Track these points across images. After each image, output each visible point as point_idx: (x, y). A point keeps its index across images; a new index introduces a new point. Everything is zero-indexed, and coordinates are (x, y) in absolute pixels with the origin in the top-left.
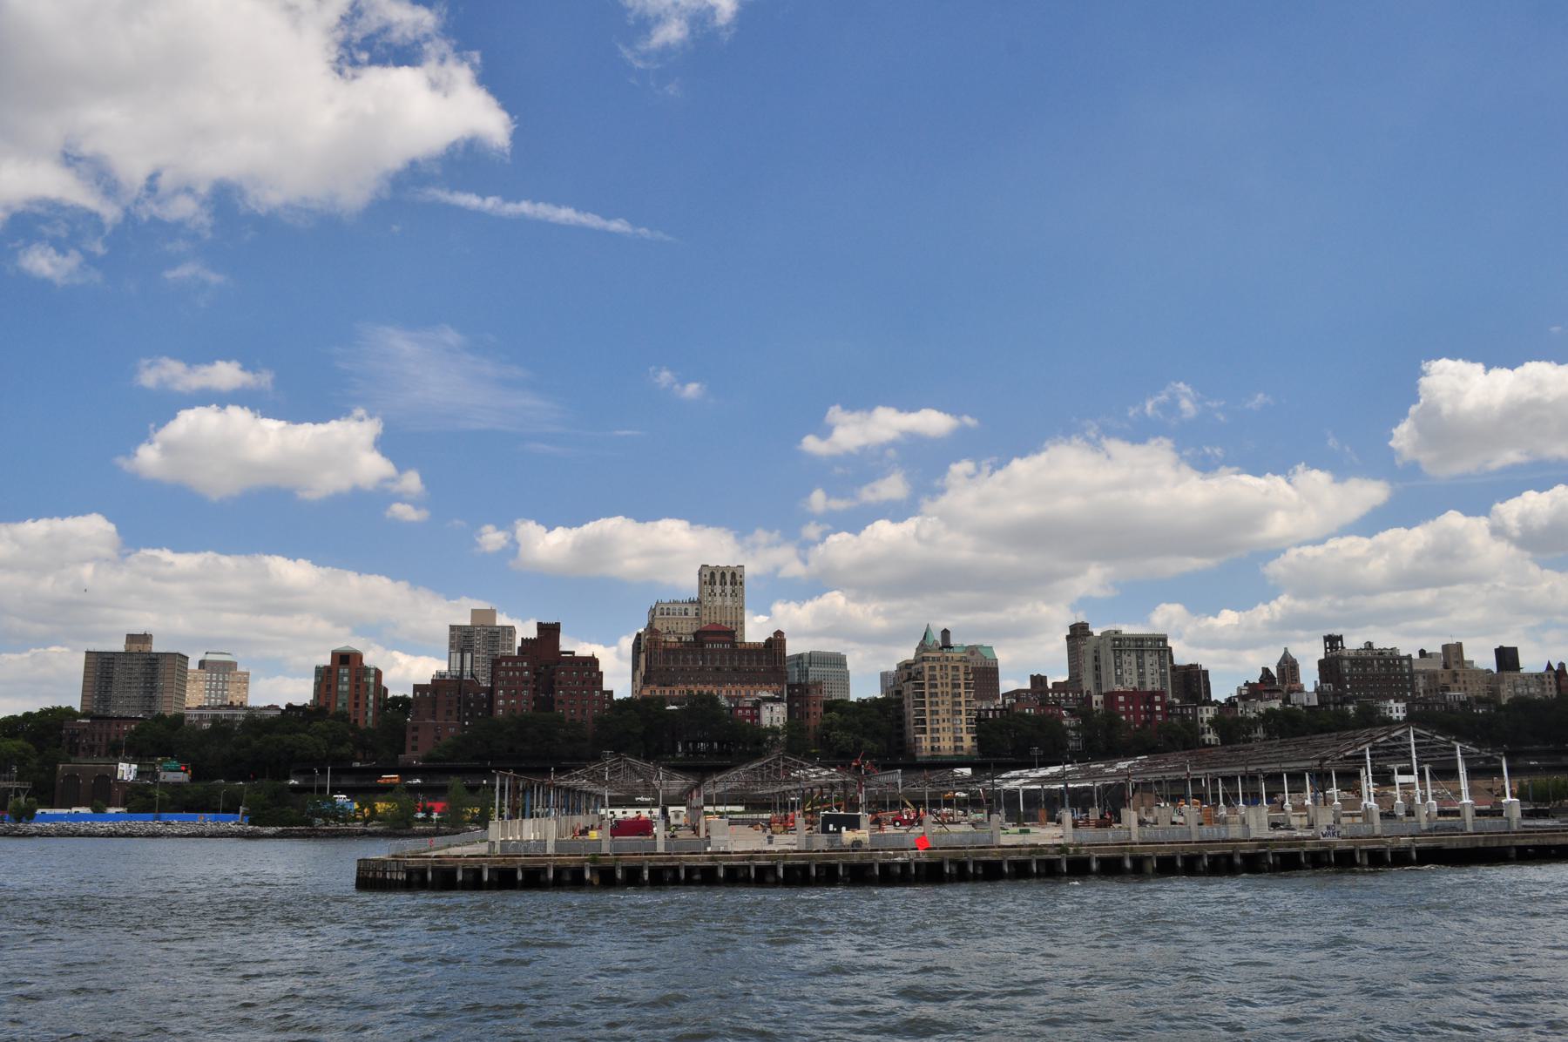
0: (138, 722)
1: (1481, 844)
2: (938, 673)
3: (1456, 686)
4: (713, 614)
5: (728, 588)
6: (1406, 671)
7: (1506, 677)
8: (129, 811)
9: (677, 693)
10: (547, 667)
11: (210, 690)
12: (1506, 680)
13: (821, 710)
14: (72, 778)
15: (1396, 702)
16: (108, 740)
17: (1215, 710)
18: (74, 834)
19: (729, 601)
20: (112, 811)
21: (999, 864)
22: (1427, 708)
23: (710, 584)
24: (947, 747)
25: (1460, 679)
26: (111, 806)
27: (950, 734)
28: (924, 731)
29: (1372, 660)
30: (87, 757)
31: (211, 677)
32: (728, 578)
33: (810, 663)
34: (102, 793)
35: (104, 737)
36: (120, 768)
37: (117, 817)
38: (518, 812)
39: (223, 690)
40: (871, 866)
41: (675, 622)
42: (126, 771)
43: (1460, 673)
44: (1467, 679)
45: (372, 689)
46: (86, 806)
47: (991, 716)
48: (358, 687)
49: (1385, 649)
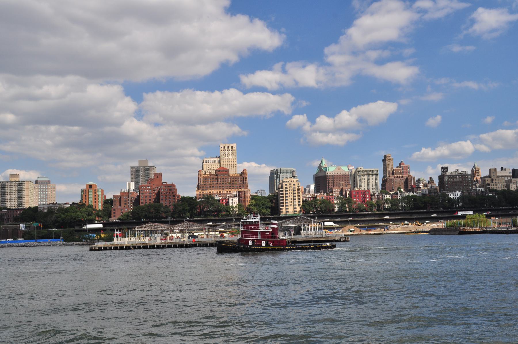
0: (23, 210)
1: (305, 240)
2: (288, 186)
3: (492, 184)
4: (225, 162)
5: (230, 152)
6: (470, 179)
7: (513, 181)
8: (25, 239)
9: (208, 193)
10: (158, 188)
11: (41, 192)
12: (513, 182)
13: (250, 199)
14: (5, 230)
15: (459, 192)
16: (13, 216)
17: (390, 196)
18: (13, 246)
19: (231, 157)
20: (19, 239)
21: (207, 244)
22: (469, 194)
23: (223, 151)
24: (291, 211)
25: (494, 181)
26: (19, 238)
27: (292, 207)
28: (283, 206)
29: (456, 176)
30: (7, 222)
31: (41, 187)
32: (230, 148)
33: (281, 173)
34: (15, 234)
35: (12, 215)
36: (20, 226)
37: (21, 241)
38: (123, 236)
39: (46, 192)
40: (183, 245)
41: (211, 165)
42: (22, 227)
43: (494, 179)
44: (497, 182)
45: (100, 196)
46: (11, 238)
47: (309, 200)
48: (95, 196)
49: (462, 172)
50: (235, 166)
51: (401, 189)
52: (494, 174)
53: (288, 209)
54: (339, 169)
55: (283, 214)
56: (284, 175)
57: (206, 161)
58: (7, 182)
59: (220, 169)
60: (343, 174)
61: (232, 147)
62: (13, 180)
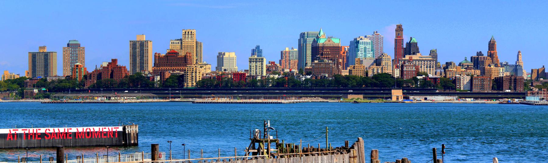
2: (189, 70)
3: (354, 70)
5: (190, 36)
28: (185, 82)
32: (190, 33)
42: (36, 91)
48: (80, 72)
50: (193, 47)
51: (106, 88)
52: (357, 62)
53: (188, 84)
54: (329, 41)
55: (185, 87)
56: (311, 39)
57: (172, 42)
58: (37, 53)
59: (170, 52)
60: (333, 45)
61: (191, 32)
62: (42, 51)
